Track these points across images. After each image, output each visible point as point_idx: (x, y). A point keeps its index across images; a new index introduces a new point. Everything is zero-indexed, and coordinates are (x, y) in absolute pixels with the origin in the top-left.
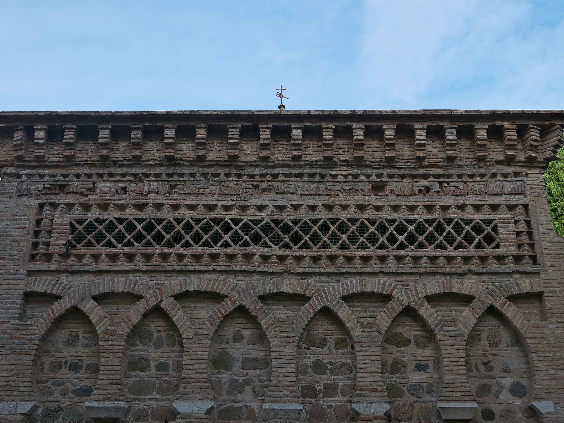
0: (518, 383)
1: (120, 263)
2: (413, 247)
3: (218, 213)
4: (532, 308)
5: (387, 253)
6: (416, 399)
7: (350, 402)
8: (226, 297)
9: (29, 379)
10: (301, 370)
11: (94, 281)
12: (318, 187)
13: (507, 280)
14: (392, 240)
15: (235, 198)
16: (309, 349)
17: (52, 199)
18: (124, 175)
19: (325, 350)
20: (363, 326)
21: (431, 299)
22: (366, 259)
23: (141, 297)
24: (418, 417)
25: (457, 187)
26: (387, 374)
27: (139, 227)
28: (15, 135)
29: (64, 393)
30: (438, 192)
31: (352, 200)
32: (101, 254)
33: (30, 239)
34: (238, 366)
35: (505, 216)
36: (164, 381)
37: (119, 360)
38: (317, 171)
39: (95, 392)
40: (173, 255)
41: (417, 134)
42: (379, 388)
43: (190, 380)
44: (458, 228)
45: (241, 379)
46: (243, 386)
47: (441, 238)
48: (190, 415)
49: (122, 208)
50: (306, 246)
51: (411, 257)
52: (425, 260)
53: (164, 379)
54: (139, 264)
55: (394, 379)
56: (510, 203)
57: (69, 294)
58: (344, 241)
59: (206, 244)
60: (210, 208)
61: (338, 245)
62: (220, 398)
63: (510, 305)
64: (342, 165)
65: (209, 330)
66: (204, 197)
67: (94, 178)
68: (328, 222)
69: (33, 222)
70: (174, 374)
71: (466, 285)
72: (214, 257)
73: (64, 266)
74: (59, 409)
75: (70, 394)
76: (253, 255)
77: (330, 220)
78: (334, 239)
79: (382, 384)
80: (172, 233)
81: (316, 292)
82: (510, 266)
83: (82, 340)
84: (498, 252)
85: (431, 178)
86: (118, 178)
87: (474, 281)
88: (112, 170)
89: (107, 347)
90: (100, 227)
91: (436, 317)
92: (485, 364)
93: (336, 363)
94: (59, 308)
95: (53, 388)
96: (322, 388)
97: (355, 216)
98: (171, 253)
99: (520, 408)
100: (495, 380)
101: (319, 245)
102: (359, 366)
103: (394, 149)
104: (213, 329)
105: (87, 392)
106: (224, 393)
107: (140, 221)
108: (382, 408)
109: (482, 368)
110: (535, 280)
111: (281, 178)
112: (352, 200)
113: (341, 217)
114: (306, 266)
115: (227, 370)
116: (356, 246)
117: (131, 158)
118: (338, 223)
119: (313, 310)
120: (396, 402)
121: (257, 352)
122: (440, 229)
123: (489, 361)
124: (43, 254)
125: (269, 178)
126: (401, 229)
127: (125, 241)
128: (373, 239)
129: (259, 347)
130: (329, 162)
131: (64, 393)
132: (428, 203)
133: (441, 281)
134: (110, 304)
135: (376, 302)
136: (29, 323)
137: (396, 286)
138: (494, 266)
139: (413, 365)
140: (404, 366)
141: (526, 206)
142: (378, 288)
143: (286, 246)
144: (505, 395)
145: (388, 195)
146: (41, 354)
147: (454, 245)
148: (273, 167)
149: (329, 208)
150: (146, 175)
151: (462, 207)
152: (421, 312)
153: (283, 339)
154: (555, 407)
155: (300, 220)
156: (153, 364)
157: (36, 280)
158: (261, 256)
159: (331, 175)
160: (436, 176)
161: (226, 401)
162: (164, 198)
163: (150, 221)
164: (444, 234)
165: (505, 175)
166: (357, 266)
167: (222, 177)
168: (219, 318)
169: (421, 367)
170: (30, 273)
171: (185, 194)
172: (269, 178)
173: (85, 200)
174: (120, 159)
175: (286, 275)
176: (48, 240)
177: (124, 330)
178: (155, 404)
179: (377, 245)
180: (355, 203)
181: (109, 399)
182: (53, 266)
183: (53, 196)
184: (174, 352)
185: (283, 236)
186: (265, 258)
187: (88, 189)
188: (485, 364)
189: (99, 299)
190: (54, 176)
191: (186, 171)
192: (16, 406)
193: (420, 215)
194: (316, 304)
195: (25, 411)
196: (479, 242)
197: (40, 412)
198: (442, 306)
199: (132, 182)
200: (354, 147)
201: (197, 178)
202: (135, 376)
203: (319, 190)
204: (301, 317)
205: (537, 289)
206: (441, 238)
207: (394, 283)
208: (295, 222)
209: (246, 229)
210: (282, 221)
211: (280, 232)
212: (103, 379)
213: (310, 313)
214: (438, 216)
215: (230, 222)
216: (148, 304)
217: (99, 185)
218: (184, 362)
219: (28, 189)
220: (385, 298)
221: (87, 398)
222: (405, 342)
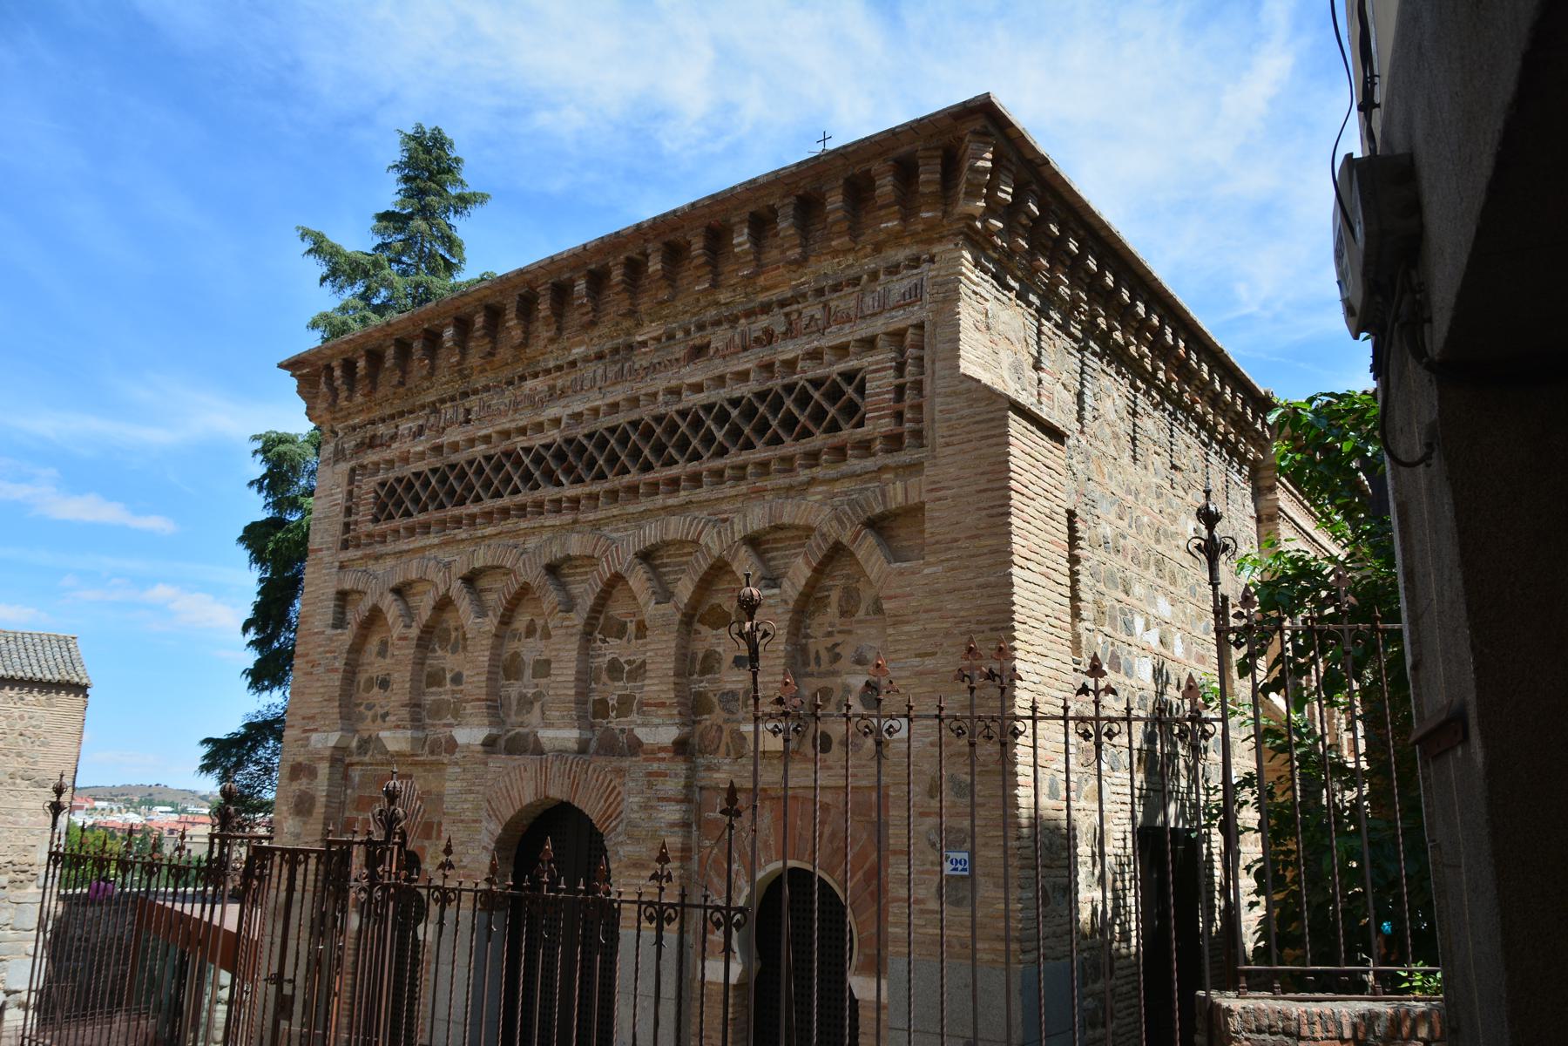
6: (726, 716)
10: (585, 677)
16: (604, 641)
22: (674, 484)
26: (695, 676)
31: (660, 383)
33: (342, 518)
34: (528, 672)
35: (881, 357)
45: (530, 692)
46: (532, 703)
48: (468, 746)
50: (601, 476)
51: (733, 468)
58: (646, 458)
60: (506, 434)
63: (865, 537)
87: (819, 497)
93: (634, 661)
95: (367, 712)
97: (662, 410)
100: (839, 680)
106: (513, 713)
108: (665, 734)
112: (660, 383)
123: (836, 645)
126: (723, 417)
143: (579, 480)
149: (634, 402)
151: (815, 355)
156: (448, 676)
158: (551, 501)
159: (639, 343)
160: (783, 304)
173: (387, 454)
180: (665, 384)
193: (745, 390)
196: (834, 420)
202: (433, 694)
205: (914, 499)
209: (538, 460)
219: (343, 449)
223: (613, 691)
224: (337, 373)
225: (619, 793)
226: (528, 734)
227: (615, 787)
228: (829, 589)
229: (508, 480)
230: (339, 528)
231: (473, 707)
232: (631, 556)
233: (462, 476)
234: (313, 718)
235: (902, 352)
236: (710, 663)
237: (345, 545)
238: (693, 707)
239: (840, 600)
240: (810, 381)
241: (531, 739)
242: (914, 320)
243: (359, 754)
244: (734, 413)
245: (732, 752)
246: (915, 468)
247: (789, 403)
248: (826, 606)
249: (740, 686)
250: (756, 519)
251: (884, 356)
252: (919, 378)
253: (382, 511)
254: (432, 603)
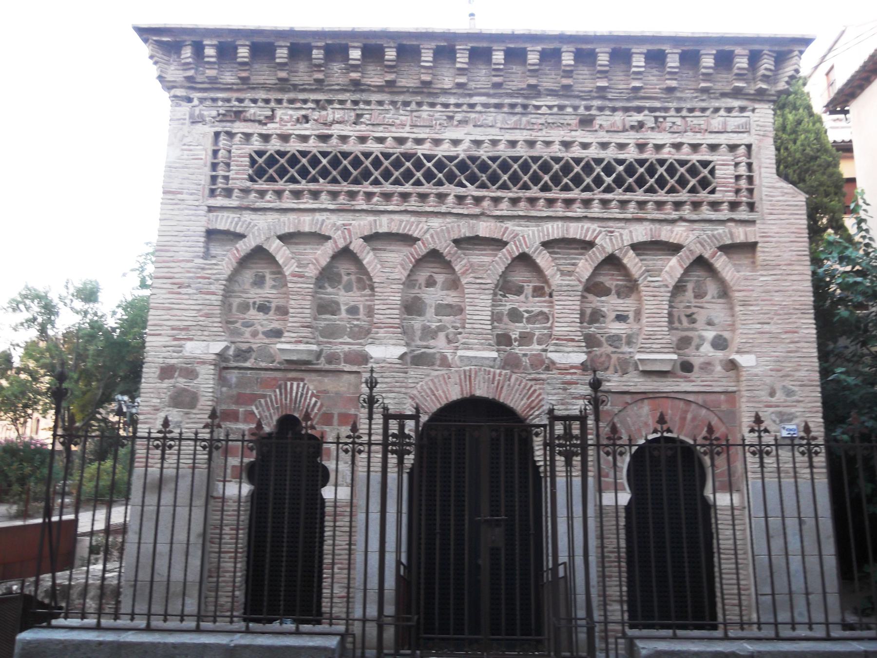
0: (721, 336)
1: (305, 200)
2: (620, 190)
3: (409, 146)
4: (744, 260)
5: (592, 197)
7: (545, 351)
8: (418, 239)
9: (218, 320)
10: (496, 318)
11: (279, 220)
12: (520, 120)
13: (720, 230)
14: (598, 181)
15: (427, 130)
16: (504, 296)
17: (228, 127)
18: (305, 101)
19: (522, 298)
20: (563, 273)
21: (638, 248)
22: (568, 202)
23: (328, 238)
24: (615, 367)
25: (674, 123)
26: (585, 324)
27: (324, 161)
28: (183, 52)
29: (255, 334)
30: (652, 128)
31: (557, 135)
32: (284, 191)
33: (207, 171)
34: (430, 312)
36: (356, 326)
37: (309, 303)
38: (519, 101)
39: (286, 334)
40: (361, 193)
41: (634, 59)
42: (577, 338)
43: (383, 325)
44: (671, 170)
45: (434, 325)
47: (652, 181)
48: (384, 361)
49: (304, 138)
50: (504, 187)
51: (618, 201)
52: (632, 205)
53: (356, 323)
54: (325, 201)
55: (592, 329)
56: (731, 142)
57: (253, 233)
58: (546, 183)
59: (397, 182)
60: (401, 141)
61: (540, 186)
62: (413, 344)
63: (720, 256)
64: (548, 95)
65: (401, 274)
66: (393, 129)
67: (273, 104)
68: (530, 161)
69: (210, 153)
70: (365, 318)
71: (675, 233)
72: (405, 196)
73: (245, 203)
74: (250, 350)
75: (261, 336)
76: (447, 195)
77: (531, 157)
78: (536, 179)
79: (579, 333)
80: (360, 170)
81: (514, 237)
82: (725, 213)
83: (269, 282)
85: (646, 112)
86: (298, 105)
87: (684, 229)
88: (292, 95)
89: (295, 289)
90: (282, 161)
91: (641, 267)
92: (688, 316)
93: (532, 311)
94: (244, 247)
96: (517, 336)
97: (560, 155)
98: (359, 192)
99: (721, 361)
100: (696, 333)
101: (519, 186)
102: (556, 315)
103: (606, 77)
104: (406, 273)
105: (277, 334)
106: (417, 338)
107: (325, 154)
108: (580, 358)
109: (685, 320)
110: (750, 229)
111: (479, 108)
112: (557, 135)
113: (543, 154)
114: (504, 208)
115: (420, 315)
116: (559, 188)
117: (312, 82)
118: (540, 162)
119: (511, 255)
120: (594, 353)
121: (451, 298)
122: (651, 171)
123: (693, 314)
124: (223, 189)
125: (465, 108)
126: (609, 170)
127: (309, 177)
128: (577, 181)
129: (453, 293)
130: (534, 91)
131: (255, 334)
132: (641, 141)
133: (649, 228)
134: (296, 244)
135: (577, 249)
136: (214, 262)
137: (600, 233)
138: (706, 212)
139: (613, 315)
140: (603, 317)
141: (749, 147)
142: (581, 234)
143: (483, 186)
144: (707, 349)
145: (596, 131)
146: (228, 295)
147: (666, 189)
148: (471, 96)
149: (531, 144)
150: (330, 102)
151: (677, 146)
152: (625, 261)
153: (478, 286)
154: (757, 361)
155: (498, 157)
156: (343, 308)
157: (217, 217)
158: (456, 196)
160: (652, 110)
161: (418, 347)
162: (351, 129)
163: (336, 156)
164: (656, 176)
165: (729, 110)
166: (559, 210)
167: (413, 106)
168: (411, 262)
169: (621, 318)
170: (211, 209)
171: (373, 125)
172: (465, 108)
173: (264, 130)
174: (301, 83)
175: (483, 218)
176: (227, 174)
177: (312, 272)
178: (346, 348)
179: (582, 187)
180: (561, 139)
181: (300, 342)
182: (234, 202)
183: (229, 124)
184: (365, 296)
185: (479, 174)
186: (460, 199)
187: (267, 117)
188: (688, 316)
189: (285, 238)
190: (228, 100)
191: (375, 97)
192: (208, 346)
193: (631, 154)
194: (513, 250)
195: (217, 351)
196: (694, 187)
197: (231, 352)
198: (647, 255)
199: (313, 109)
200: (562, 74)
201: (386, 107)
202: (325, 320)
203: (520, 124)
204: (497, 263)
206: (652, 181)
207: (598, 229)
208: (494, 159)
209: (440, 165)
210: (479, 157)
211: (476, 170)
212: (292, 321)
213: (507, 259)
214: (649, 155)
215: (422, 157)
216: (337, 246)
217: (279, 113)
218: (376, 307)
219: (201, 116)
220: (587, 245)
221: (278, 340)
222: (606, 292)
223: (516, 330)
225: (540, 394)
226: (435, 354)
227: (535, 391)
228: (686, 281)
231: (386, 332)
232: (537, 243)
234: (186, 329)
236: (596, 316)
238: (591, 341)
239: (694, 289)
240: (678, 161)
241: (438, 356)
242: (747, 142)
243: (238, 361)
245: (619, 371)
246: (752, 222)
247: (661, 170)
248: (685, 291)
249: (623, 332)
254: (331, 253)
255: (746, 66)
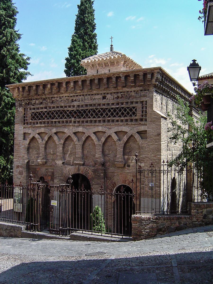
30: (121, 98)
60: (62, 107)
84: (136, 118)
98: (53, 121)
132: (118, 102)
151: (127, 103)
168: (64, 139)
209: (70, 113)
224: (21, 89)
229: (64, 116)
230: (23, 120)
233: (53, 113)
235: (143, 105)
237: (24, 124)
244: (112, 111)
250: (116, 129)
251: (139, 106)
252: (146, 110)
253: (33, 118)
255: (142, 78)
